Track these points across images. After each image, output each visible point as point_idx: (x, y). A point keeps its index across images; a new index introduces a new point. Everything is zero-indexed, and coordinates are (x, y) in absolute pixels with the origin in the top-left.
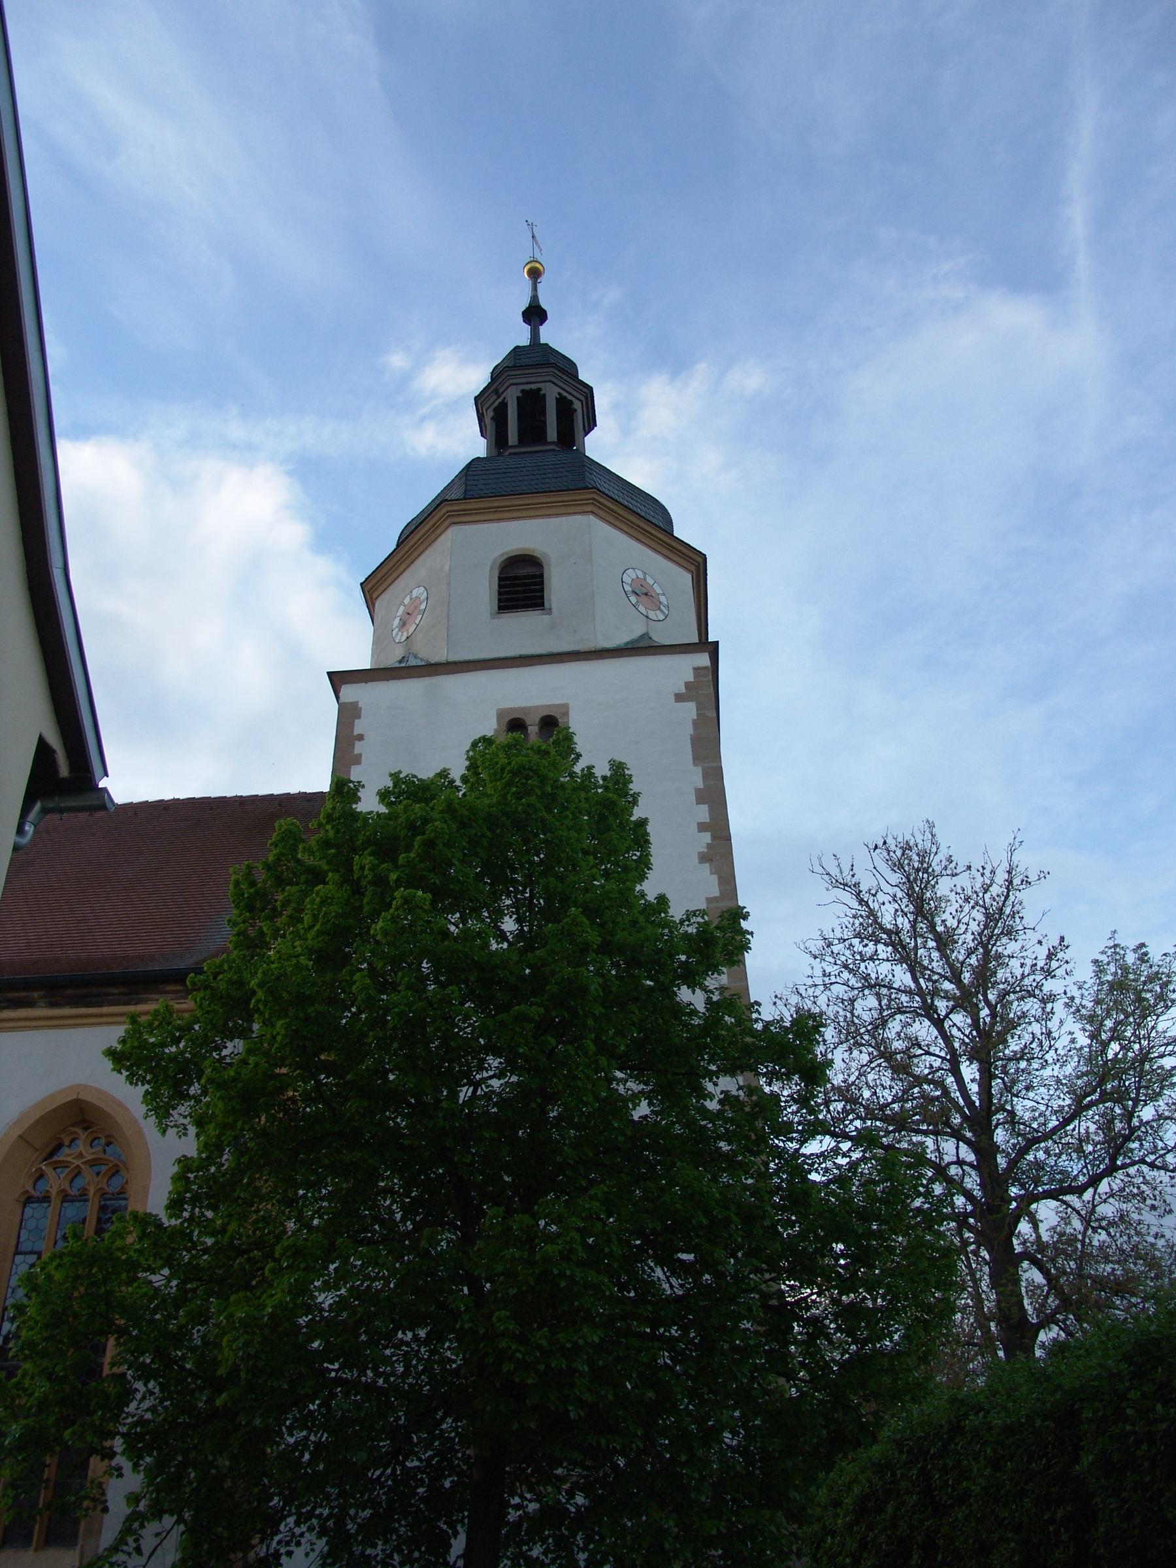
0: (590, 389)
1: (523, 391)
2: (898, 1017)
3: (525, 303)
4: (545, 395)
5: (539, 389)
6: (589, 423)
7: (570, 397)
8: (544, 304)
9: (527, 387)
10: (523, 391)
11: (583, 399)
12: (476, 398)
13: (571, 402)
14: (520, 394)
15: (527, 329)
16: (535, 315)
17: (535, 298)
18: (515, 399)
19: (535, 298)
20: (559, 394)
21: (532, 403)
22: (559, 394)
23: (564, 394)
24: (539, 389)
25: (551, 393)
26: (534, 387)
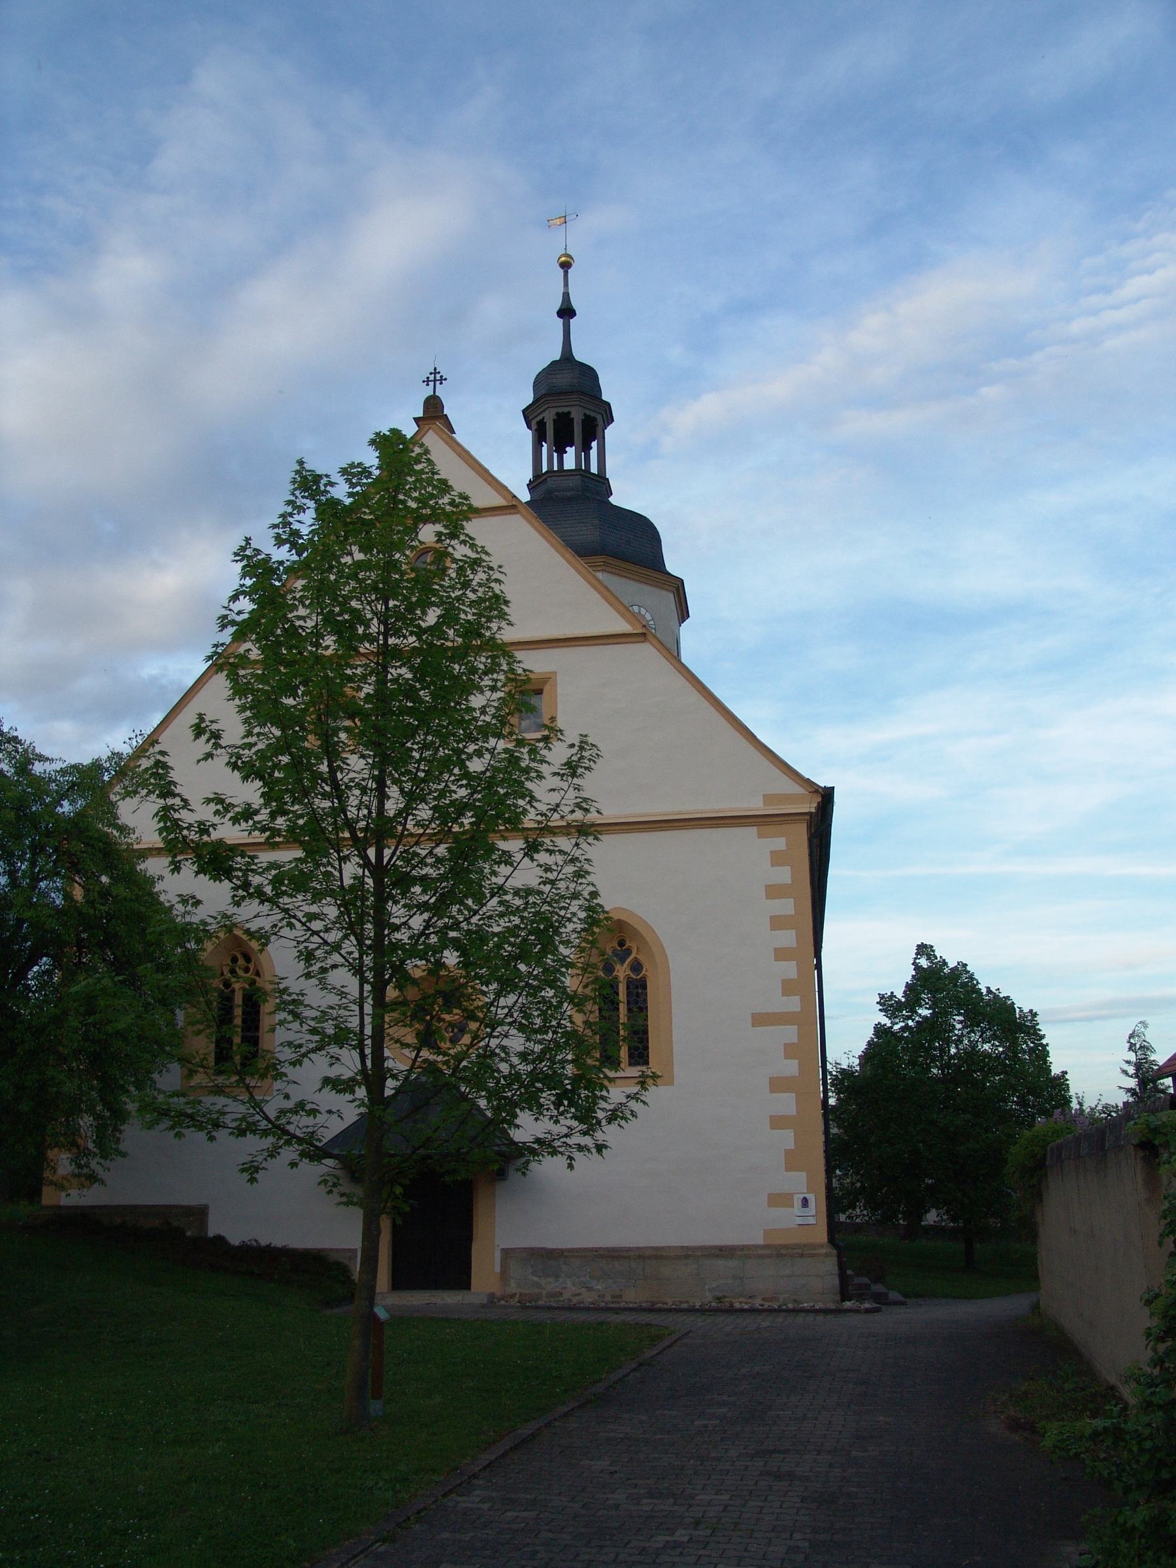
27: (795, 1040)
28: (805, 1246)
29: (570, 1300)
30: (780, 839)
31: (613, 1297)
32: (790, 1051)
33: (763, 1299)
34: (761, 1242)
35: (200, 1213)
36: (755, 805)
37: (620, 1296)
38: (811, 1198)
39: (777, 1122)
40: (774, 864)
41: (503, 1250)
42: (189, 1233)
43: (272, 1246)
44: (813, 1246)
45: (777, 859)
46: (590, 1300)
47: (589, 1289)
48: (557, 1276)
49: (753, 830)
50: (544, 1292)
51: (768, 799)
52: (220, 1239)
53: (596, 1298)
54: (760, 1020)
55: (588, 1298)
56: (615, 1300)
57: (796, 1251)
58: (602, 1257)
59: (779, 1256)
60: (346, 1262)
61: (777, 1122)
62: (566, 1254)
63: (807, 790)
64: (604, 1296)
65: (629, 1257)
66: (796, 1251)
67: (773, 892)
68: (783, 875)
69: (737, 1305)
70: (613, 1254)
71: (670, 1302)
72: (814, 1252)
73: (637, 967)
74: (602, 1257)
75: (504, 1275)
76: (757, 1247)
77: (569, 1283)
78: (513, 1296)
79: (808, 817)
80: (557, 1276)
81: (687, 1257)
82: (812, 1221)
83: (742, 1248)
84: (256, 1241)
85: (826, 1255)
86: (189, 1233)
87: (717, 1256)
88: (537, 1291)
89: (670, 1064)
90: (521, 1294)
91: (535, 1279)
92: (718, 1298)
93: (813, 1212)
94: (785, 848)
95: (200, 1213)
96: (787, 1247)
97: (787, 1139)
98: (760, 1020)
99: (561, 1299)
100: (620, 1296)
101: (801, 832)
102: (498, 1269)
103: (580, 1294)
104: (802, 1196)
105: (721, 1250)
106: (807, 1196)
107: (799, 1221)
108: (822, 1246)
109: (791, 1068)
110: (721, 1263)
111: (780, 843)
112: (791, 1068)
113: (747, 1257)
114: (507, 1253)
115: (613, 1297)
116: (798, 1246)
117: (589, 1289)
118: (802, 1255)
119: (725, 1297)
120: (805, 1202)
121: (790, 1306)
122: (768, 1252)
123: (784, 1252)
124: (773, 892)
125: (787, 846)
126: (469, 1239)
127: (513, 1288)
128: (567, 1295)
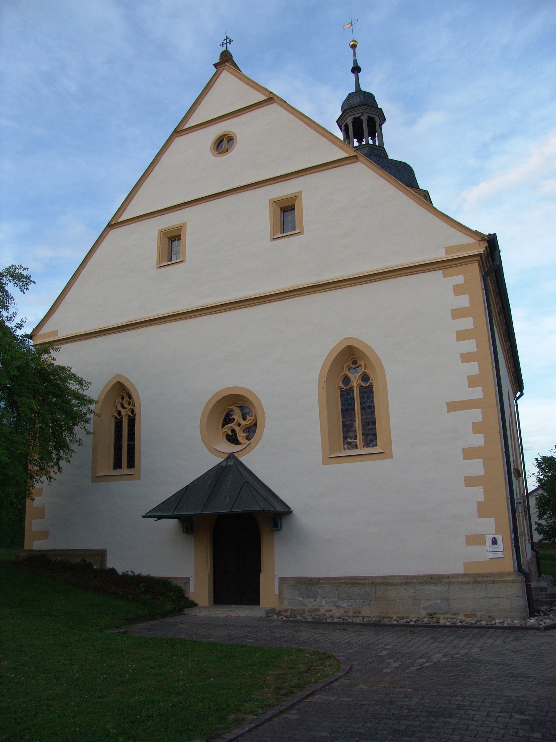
0: (381, 109)
1: (354, 118)
3: (351, 66)
4: (362, 119)
7: (373, 116)
8: (360, 64)
9: (355, 116)
13: (374, 118)
16: (356, 70)
17: (355, 61)
19: (355, 61)
20: (368, 116)
21: (357, 122)
22: (368, 116)
23: (370, 115)
27: (480, 419)
28: (496, 574)
29: (324, 615)
30: (459, 276)
31: (354, 613)
32: (477, 428)
33: (465, 616)
34: (462, 571)
35: (102, 554)
36: (441, 255)
37: (359, 612)
38: (499, 537)
39: (470, 481)
40: (456, 294)
41: (280, 578)
42: (95, 567)
43: (141, 575)
44: (502, 575)
45: (458, 290)
46: (338, 614)
47: (338, 607)
48: (315, 598)
49: (440, 273)
50: (307, 609)
51: (448, 250)
52: (113, 571)
53: (343, 613)
54: (453, 407)
55: (337, 613)
56: (355, 615)
57: (489, 579)
58: (346, 583)
59: (476, 582)
60: (182, 586)
61: (470, 481)
62: (321, 581)
63: (475, 240)
64: (348, 612)
65: (364, 584)
66: (489, 579)
67: (457, 314)
68: (464, 301)
69: (442, 621)
70: (354, 582)
71: (395, 617)
72: (502, 579)
73: (365, 377)
74: (346, 583)
75: (281, 597)
76: (458, 575)
77: (324, 602)
78: (286, 611)
79: (479, 258)
80: (315, 598)
81: (407, 584)
82: (500, 555)
83: (447, 577)
84: (132, 572)
85: (513, 581)
86: (95, 567)
87: (429, 583)
88: (302, 607)
89: (389, 444)
90: (292, 610)
91: (301, 599)
92: (431, 615)
93: (501, 548)
94: (463, 282)
95: (102, 554)
96: (482, 575)
97: (478, 493)
98: (453, 407)
99: (318, 613)
100: (359, 612)
101: (474, 270)
102: (277, 592)
103: (331, 611)
104: (492, 537)
105: (432, 578)
106: (496, 536)
107: (490, 555)
108: (509, 574)
109: (478, 440)
110: (432, 587)
111: (459, 279)
112: (478, 440)
113: (451, 583)
114: (282, 580)
115: (354, 613)
116: (490, 575)
117: (338, 607)
118: (494, 582)
119: (435, 613)
120: (494, 541)
121: (484, 623)
122: (467, 579)
123: (479, 579)
124: (457, 314)
125: (465, 280)
126: (258, 570)
127: (286, 605)
128: (322, 611)
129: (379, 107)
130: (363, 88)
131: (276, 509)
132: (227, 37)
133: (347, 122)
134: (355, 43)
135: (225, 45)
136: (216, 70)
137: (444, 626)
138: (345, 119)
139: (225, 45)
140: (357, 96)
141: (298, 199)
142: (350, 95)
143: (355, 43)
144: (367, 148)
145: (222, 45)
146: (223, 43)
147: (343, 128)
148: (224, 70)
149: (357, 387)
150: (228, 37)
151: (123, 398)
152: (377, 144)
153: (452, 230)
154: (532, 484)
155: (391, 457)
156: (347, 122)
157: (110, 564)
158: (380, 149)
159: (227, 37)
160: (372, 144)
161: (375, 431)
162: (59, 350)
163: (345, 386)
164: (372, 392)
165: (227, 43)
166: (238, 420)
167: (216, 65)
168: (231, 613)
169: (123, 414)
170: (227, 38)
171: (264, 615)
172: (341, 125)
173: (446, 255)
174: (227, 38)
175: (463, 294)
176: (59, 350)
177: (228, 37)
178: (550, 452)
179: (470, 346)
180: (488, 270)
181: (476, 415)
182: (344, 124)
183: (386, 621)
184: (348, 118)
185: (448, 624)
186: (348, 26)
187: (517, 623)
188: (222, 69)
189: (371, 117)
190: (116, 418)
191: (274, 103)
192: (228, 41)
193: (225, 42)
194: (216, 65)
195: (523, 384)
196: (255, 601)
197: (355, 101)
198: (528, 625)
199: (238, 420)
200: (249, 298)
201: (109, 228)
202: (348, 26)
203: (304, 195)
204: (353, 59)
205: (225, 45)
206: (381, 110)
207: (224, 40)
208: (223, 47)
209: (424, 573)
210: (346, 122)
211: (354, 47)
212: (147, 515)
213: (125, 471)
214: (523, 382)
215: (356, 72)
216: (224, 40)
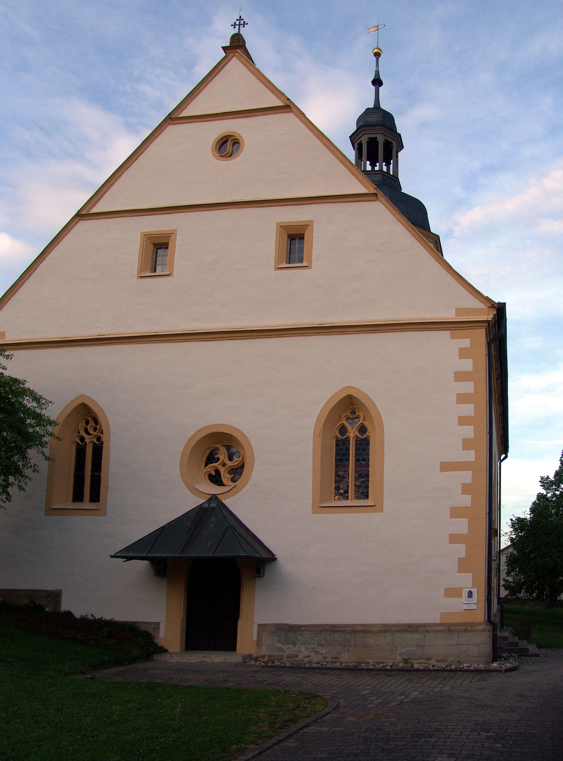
0: (400, 134)
1: (369, 138)
2: (424, 682)
5: (376, 138)
6: (400, 147)
7: (390, 140)
9: (371, 136)
10: (369, 138)
11: (396, 139)
12: (350, 137)
13: (391, 143)
14: (368, 140)
15: (373, 88)
17: (377, 73)
18: (366, 143)
19: (377, 73)
20: (385, 140)
21: (372, 143)
22: (385, 140)
23: (387, 139)
24: (376, 138)
25: (381, 139)
26: (374, 136)
27: (470, 481)
28: (469, 624)
29: (303, 660)
30: (465, 340)
31: (332, 658)
32: (466, 489)
33: (437, 661)
34: (438, 621)
35: (56, 596)
36: (451, 316)
37: (338, 658)
38: (475, 591)
39: (454, 539)
40: (461, 357)
41: (259, 625)
43: (103, 619)
44: (473, 624)
45: (463, 353)
46: (316, 660)
47: (317, 653)
48: (294, 644)
49: (448, 333)
50: (285, 655)
51: (459, 311)
52: (69, 614)
53: (321, 659)
54: (446, 467)
55: (315, 658)
56: (333, 660)
57: (461, 628)
58: (326, 630)
59: (450, 631)
60: (151, 631)
61: (454, 539)
62: (301, 628)
63: (485, 305)
64: (326, 658)
65: (345, 631)
66: (461, 628)
67: (460, 376)
68: (467, 365)
69: (416, 666)
70: (334, 629)
71: (371, 662)
72: (473, 628)
73: (363, 429)
74: (326, 630)
75: (259, 643)
76: (434, 624)
77: (303, 648)
78: (263, 657)
79: (486, 325)
80: (294, 644)
81: (385, 631)
82: (474, 607)
83: (425, 625)
84: (92, 615)
85: (483, 630)
87: (406, 631)
88: (281, 653)
89: (381, 498)
90: (270, 656)
91: (280, 645)
92: (406, 660)
93: (475, 601)
94: (469, 346)
95: (56, 596)
96: (456, 625)
97: (460, 550)
98: (446, 467)
99: (297, 659)
100: (338, 658)
101: (481, 335)
102: (255, 638)
103: (310, 656)
104: (469, 590)
105: (409, 627)
106: (472, 590)
107: (465, 607)
108: (480, 624)
109: (466, 501)
110: (409, 635)
111: (465, 343)
112: (466, 501)
113: (427, 631)
114: (261, 627)
115: (332, 658)
116: (463, 624)
117: (317, 653)
118: (465, 631)
119: (410, 659)
120: (470, 594)
121: (453, 667)
122: (442, 628)
123: (453, 628)
124: (460, 376)
125: (471, 345)
126: (236, 616)
127: (264, 651)
128: (300, 657)
129: (398, 132)
130: (383, 106)
131: (261, 556)
132: (240, 17)
133: (361, 141)
134: (379, 51)
135: (238, 26)
136: (225, 55)
137: (418, 670)
138: (358, 137)
139: (237, 27)
140: (376, 114)
141: (308, 228)
142: (368, 110)
143: (379, 51)
144: (381, 175)
145: (234, 25)
146: (235, 23)
147: (356, 147)
148: (234, 57)
149: (353, 438)
150: (242, 18)
151: (87, 423)
152: (391, 173)
153: (464, 292)
154: (505, 542)
155: (382, 511)
156: (361, 141)
157: (65, 606)
158: (395, 179)
159: (240, 17)
160: (386, 171)
161: (367, 484)
162: (11, 358)
163: (341, 435)
164: (368, 444)
165: (240, 25)
166: (223, 460)
167: (225, 49)
168: (205, 659)
169: (87, 440)
170: (240, 19)
171: (241, 661)
172: (354, 142)
173: (456, 316)
174: (240, 19)
175: (468, 357)
176: (11, 358)
177: (242, 18)
178: (524, 513)
179: (468, 409)
180: (494, 337)
181: (467, 476)
182: (358, 142)
183: (363, 666)
184: (364, 136)
185: (421, 668)
186: (373, 29)
187: (482, 666)
188: (232, 55)
189: (388, 141)
190: (78, 444)
191: (290, 112)
192: (242, 22)
193: (238, 23)
194: (225, 49)
195: (509, 447)
196: (231, 646)
197: (373, 119)
198: (492, 668)
199: (223, 460)
200: (245, 329)
201: (78, 218)
202: (373, 29)
203: (316, 226)
204: (375, 69)
205: (237, 27)
206: (400, 135)
207: (237, 20)
208: (235, 27)
209: (402, 622)
210: (360, 141)
211: (377, 55)
212: (117, 555)
213: (87, 504)
214: (509, 445)
215: (377, 85)
216: (237, 20)
